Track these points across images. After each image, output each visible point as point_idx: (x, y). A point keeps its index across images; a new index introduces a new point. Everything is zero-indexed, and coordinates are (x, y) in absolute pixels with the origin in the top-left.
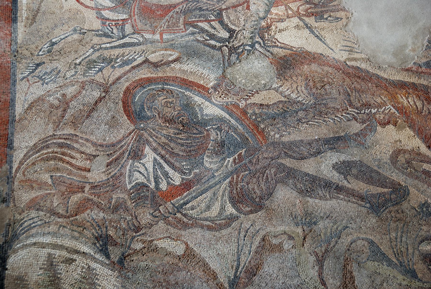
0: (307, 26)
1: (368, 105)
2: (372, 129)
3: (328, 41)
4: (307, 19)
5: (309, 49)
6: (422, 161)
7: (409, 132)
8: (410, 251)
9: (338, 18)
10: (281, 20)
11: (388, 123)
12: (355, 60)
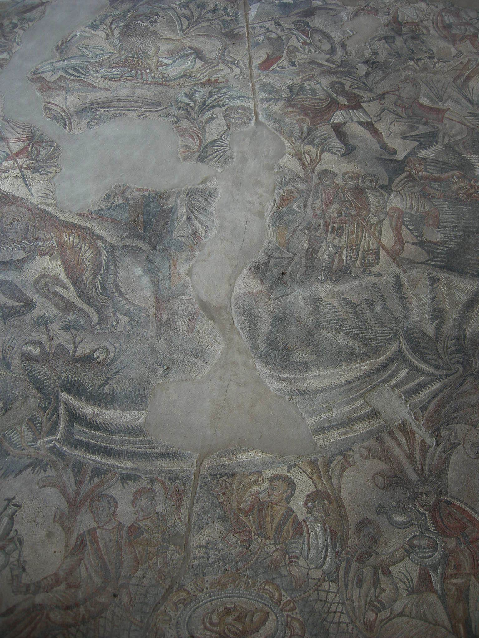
0: (24, 177)
1: (37, 239)
2: (30, 258)
3: (33, 189)
4: (25, 171)
5: (16, 194)
6: (57, 285)
7: (59, 262)
8: (15, 350)
9: (49, 172)
10: (6, 171)
11: (47, 254)
12: (46, 204)
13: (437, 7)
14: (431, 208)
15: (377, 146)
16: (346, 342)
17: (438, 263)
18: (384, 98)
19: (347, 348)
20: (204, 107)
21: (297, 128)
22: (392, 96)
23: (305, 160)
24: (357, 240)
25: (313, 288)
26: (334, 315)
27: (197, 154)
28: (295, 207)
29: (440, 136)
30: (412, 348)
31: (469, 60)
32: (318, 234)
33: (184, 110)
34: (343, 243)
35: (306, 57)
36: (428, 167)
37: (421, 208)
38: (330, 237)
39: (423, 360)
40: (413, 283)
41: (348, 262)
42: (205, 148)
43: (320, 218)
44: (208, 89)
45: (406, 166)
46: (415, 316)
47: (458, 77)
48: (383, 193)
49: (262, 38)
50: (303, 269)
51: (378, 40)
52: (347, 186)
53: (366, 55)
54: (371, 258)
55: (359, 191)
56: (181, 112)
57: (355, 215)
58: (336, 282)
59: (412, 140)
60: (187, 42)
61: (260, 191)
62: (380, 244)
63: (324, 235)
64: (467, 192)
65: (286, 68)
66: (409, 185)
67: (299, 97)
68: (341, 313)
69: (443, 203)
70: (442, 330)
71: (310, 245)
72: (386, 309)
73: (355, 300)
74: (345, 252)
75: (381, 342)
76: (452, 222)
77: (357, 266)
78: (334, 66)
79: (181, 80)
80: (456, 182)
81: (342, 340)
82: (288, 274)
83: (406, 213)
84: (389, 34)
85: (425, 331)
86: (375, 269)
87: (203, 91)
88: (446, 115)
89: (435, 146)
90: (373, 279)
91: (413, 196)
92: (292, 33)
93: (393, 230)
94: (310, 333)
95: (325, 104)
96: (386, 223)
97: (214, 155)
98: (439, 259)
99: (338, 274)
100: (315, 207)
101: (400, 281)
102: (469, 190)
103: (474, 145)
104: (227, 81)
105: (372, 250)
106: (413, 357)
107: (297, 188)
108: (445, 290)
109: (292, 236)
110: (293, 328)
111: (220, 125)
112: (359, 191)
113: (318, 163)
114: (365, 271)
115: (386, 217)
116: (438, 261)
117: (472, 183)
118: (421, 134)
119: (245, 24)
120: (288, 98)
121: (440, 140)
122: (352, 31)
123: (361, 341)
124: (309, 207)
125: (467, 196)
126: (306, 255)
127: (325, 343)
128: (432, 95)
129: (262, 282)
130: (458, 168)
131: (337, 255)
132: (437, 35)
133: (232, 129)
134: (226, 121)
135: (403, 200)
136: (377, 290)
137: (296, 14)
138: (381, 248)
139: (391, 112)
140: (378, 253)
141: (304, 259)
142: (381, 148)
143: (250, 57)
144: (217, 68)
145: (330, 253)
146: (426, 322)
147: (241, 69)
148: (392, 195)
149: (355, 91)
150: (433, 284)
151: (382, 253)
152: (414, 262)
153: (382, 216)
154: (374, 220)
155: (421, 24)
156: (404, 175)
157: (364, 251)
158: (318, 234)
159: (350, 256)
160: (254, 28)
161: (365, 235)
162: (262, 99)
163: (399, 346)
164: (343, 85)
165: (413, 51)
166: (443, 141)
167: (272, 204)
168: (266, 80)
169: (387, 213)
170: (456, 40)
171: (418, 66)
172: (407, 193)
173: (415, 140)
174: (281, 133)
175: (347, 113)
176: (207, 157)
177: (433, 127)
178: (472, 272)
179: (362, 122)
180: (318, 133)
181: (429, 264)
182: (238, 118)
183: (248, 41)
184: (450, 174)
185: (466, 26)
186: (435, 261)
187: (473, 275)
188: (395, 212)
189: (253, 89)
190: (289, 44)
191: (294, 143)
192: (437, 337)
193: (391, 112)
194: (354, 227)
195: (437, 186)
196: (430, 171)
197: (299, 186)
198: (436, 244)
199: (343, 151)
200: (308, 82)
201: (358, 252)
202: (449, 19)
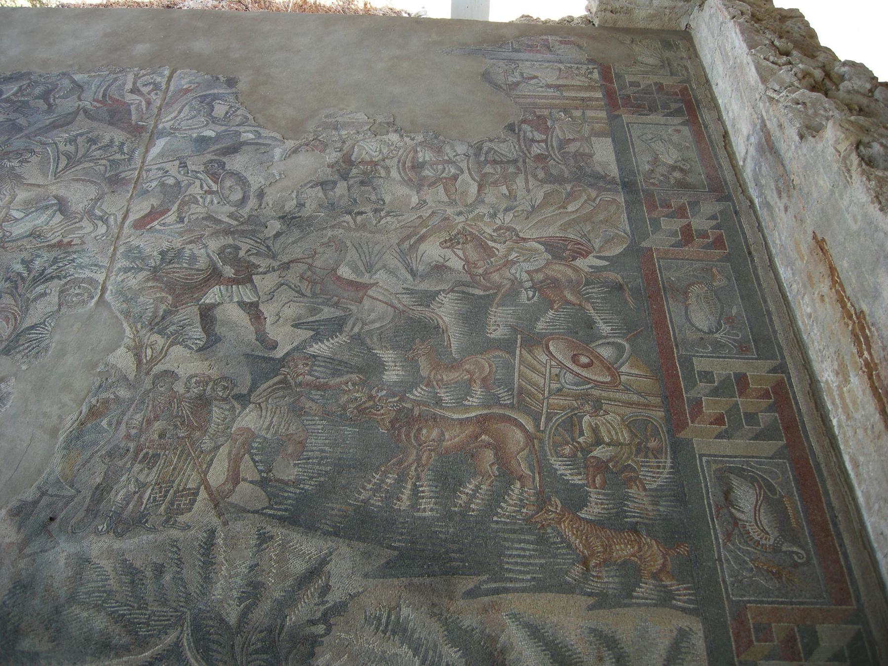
13: (413, 139)
14: (297, 429)
15: (253, 337)
16: (103, 626)
17: (279, 513)
18: (288, 268)
19: (103, 635)
20: (43, 277)
21: (151, 308)
22: (300, 265)
24: (173, 475)
25: (85, 543)
26: (100, 584)
27: (5, 344)
28: (104, 423)
29: (350, 322)
30: (196, 642)
31: (433, 213)
32: (120, 463)
33: (11, 282)
34: (152, 477)
35: (203, 210)
36: (315, 368)
37: (282, 430)
40: (232, 542)
42: (18, 335)
43: (133, 440)
44: (54, 254)
45: (284, 367)
46: (217, 592)
47: (409, 237)
49: (154, 184)
50: (81, 514)
51: (312, 187)
52: (188, 395)
53: (286, 208)
55: (203, 403)
56: (8, 284)
57: (183, 438)
58: (119, 535)
60: (54, 190)
61: (66, 398)
62: (204, 482)
63: (128, 465)
65: (169, 225)
66: (277, 395)
67: (171, 266)
68: (111, 582)
69: (318, 422)
71: (104, 479)
72: (179, 580)
73: (138, 564)
76: (322, 451)
77: (159, 512)
78: (235, 223)
79: (25, 242)
80: (350, 390)
81: (100, 623)
82: (58, 521)
84: (330, 178)
85: (224, 616)
86: (181, 519)
87: (46, 256)
88: (370, 292)
90: (175, 533)
91: (278, 411)
92: (197, 178)
94: (57, 610)
95: (202, 277)
96: (224, 450)
97: (26, 345)
98: (283, 507)
99: (124, 524)
102: (364, 403)
103: (395, 336)
104: (83, 243)
105: (189, 489)
106: (193, 657)
107: (117, 396)
108: (276, 555)
109: (84, 465)
110: (37, 601)
111: (50, 303)
112: (203, 403)
114: (167, 521)
116: (279, 510)
117: (373, 392)
118: (325, 320)
119: (139, 166)
120: (154, 268)
121: (347, 329)
122: (280, 174)
123: (125, 626)
124: (123, 425)
126: (94, 494)
128: (359, 263)
129: (19, 529)
130: (360, 371)
132: (398, 178)
133: (64, 309)
134: (59, 298)
136: (175, 549)
137: (213, 151)
138: (202, 487)
139: (290, 287)
140: (196, 494)
141: (88, 500)
142: (257, 340)
143: (128, 211)
144: (77, 225)
145: (128, 491)
146: (231, 602)
147: (108, 227)
149: (252, 259)
150: (260, 545)
151: (203, 494)
152: (244, 510)
155: (382, 163)
156: (276, 379)
157: (177, 491)
158: (120, 463)
160: (149, 170)
162: (119, 269)
163: (178, 638)
164: (238, 248)
165: (355, 200)
166: (352, 330)
167: (76, 417)
168: (136, 243)
169: (230, 436)
170: (423, 185)
171: (355, 221)
172: (270, 407)
173: (308, 329)
174: (126, 317)
175: (227, 290)
176: (16, 348)
177: (345, 309)
178: (326, 527)
179: (244, 302)
180: (176, 319)
182: (78, 294)
183: (134, 187)
184: (345, 378)
185: (446, 165)
187: (326, 533)
189: (114, 254)
190: (188, 193)
191: (138, 332)
192: (239, 626)
193: (290, 287)
196: (316, 374)
197: (123, 393)
198: (286, 483)
200: (190, 246)
201: (167, 492)
202: (425, 155)
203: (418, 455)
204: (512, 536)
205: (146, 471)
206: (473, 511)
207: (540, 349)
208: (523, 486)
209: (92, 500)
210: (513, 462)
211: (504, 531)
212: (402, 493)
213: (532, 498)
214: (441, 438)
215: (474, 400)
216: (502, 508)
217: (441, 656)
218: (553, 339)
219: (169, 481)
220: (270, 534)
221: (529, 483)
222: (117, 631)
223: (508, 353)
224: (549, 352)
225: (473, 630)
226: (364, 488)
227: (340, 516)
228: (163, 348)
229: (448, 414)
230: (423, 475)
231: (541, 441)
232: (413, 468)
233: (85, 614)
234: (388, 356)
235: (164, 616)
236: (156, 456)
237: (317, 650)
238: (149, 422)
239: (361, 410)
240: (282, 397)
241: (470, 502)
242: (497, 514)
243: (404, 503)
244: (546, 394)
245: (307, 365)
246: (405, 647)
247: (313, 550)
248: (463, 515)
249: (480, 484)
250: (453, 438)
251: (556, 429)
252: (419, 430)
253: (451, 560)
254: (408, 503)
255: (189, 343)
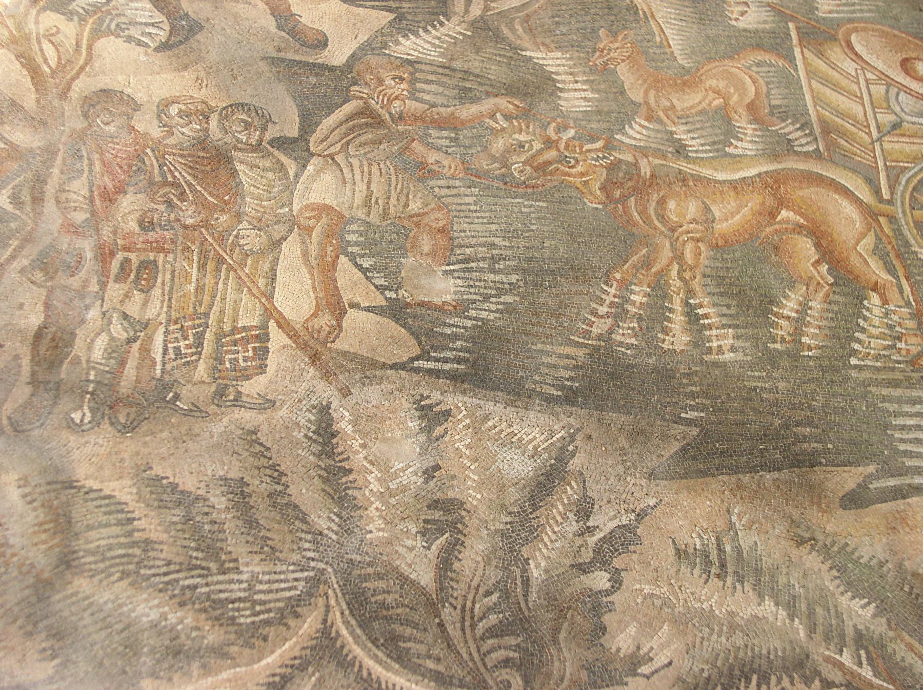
15: (270, 24)
16: (154, 615)
19: (160, 634)
23: (39, 60)
32: (75, 282)
34: (155, 309)
38: (115, 290)
39: (399, 659)
41: (168, 367)
48: (284, 159)
52: (171, 141)
54: (244, 355)
57: (194, 227)
59: (373, 7)
62: (270, 312)
63: (94, 287)
64: (533, 157)
66: (363, 138)
70: (456, 565)
71: (47, 317)
73: (189, 483)
74: (159, 339)
75: (269, 611)
77: (196, 378)
80: (503, 129)
83: (352, 220)
86: (252, 387)
89: (442, 24)
90: (247, 417)
91: (375, 169)
93: (311, 268)
96: (291, 249)
100: (67, 200)
101: (330, 422)
102: (540, 152)
105: (244, 328)
108: (468, 447)
113: (82, 68)
114: (221, 393)
115: (291, 231)
117: (551, 132)
125: (536, 169)
127: (88, 620)
130: (510, 90)
131: (136, 346)
135: (344, 182)
136: (258, 448)
138: (272, 324)
140: (264, 338)
141: (26, 362)
142: (280, 27)
145: (112, 339)
146: (409, 543)
148: (310, 168)
151: (277, 338)
153: (278, 231)
154: (251, 239)
156: (348, 108)
157: (220, 336)
159: (177, 349)
161: (225, 284)
163: (325, 621)
166: (467, 11)
169: (293, 223)
172: (355, 162)
181: (417, 370)
184: (487, 105)
186: (437, 360)
187: (549, 400)
188: (318, 218)
194: (190, 260)
195: (447, 142)
196: (427, 97)
198: (440, 309)
199: (163, 35)
201: (199, 337)
203: (673, 248)
204: (897, 392)
205: (138, 296)
206: (810, 348)
207: (838, 49)
208: (885, 302)
209: (36, 360)
210: (855, 260)
211: (879, 383)
212: (669, 320)
213: (911, 324)
214: (708, 219)
215: (745, 145)
216: (859, 341)
217: (839, 615)
218: (856, 30)
219: (195, 315)
220: (443, 407)
221: (893, 294)
222: (188, 621)
223: (779, 55)
224: (856, 54)
225: (881, 565)
226: (594, 313)
227: (566, 368)
228: (78, 45)
229: (706, 172)
230: (696, 284)
231: (892, 219)
232: (674, 273)
233: (107, 596)
234: (553, 61)
235: (281, 581)
236: (148, 267)
237: (607, 619)
238: (110, 198)
239: (542, 168)
240: (374, 142)
241: (798, 333)
242: (854, 353)
243: (677, 338)
244: (875, 134)
245: (402, 79)
246: (769, 604)
247: (536, 432)
248: (794, 356)
249: (807, 298)
250: (731, 215)
251: (912, 195)
252: (662, 202)
253: (799, 439)
254: (686, 338)
255: (135, 32)
